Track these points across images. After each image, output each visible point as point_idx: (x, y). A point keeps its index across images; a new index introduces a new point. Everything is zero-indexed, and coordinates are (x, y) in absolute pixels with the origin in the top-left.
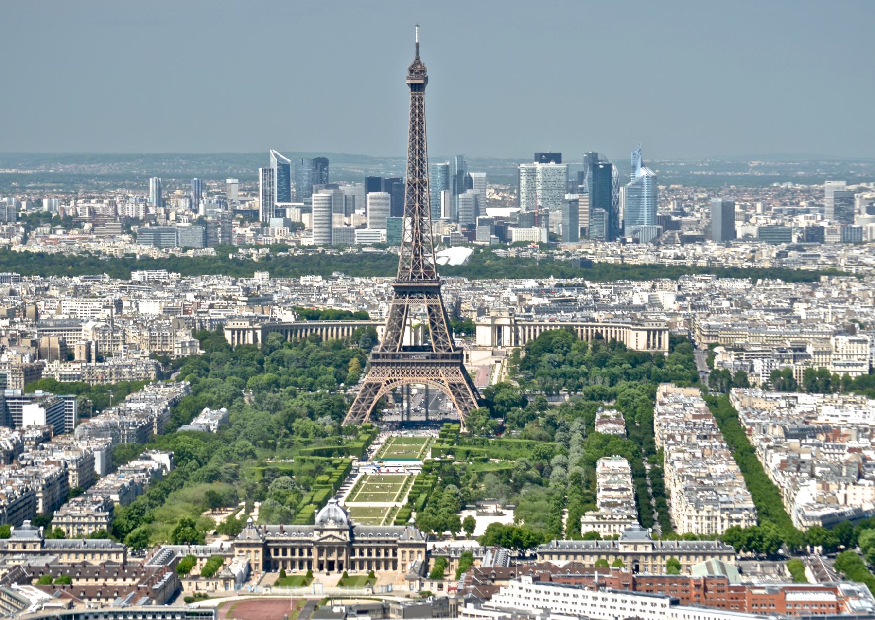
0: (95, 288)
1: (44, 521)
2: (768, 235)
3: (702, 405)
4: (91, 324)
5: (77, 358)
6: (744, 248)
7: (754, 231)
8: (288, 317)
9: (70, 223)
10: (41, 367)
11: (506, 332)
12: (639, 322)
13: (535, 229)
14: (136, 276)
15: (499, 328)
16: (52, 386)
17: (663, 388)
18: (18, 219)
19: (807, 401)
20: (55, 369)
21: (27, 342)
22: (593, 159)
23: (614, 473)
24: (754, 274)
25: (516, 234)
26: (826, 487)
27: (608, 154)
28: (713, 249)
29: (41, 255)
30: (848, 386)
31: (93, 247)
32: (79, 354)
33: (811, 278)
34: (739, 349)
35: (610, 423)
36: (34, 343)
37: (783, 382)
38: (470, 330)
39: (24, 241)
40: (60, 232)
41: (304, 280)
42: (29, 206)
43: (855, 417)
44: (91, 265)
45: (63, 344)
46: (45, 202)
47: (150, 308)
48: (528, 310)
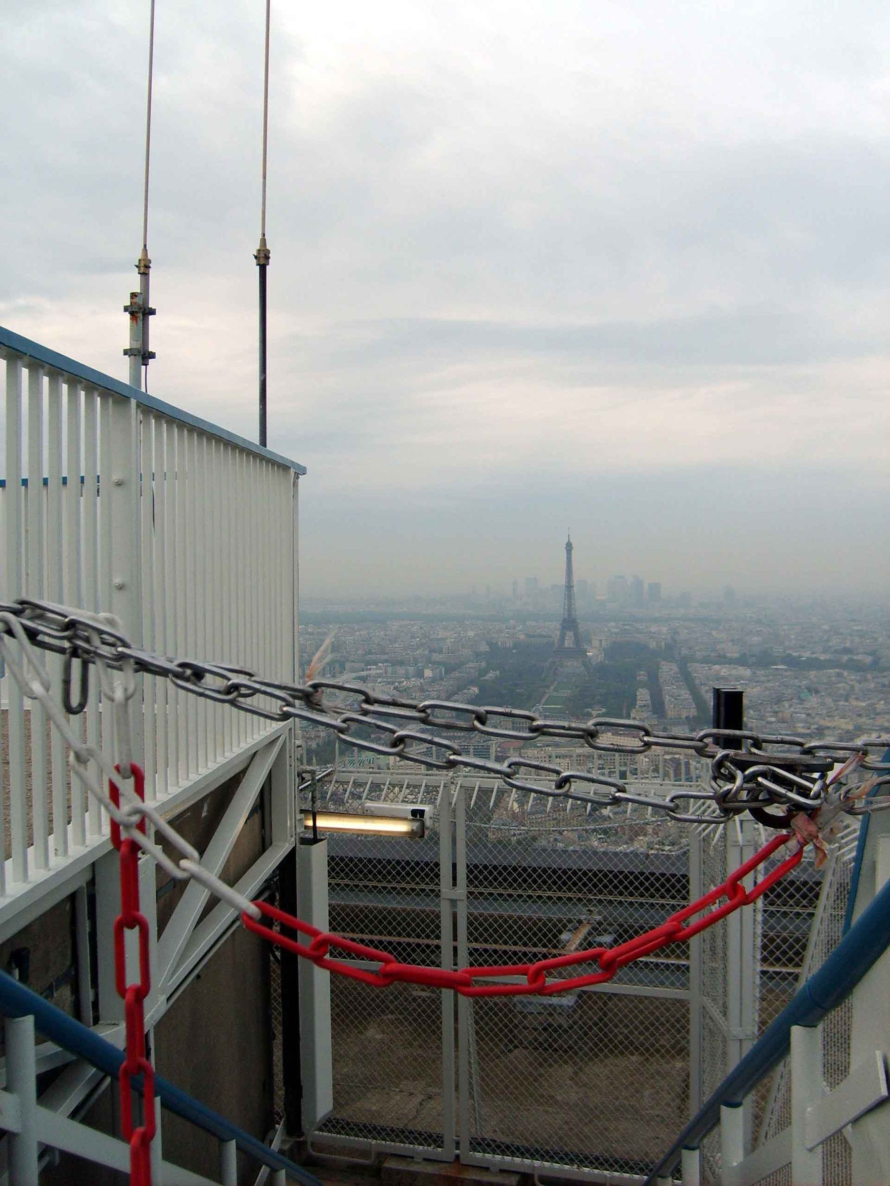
8: (522, 637)
11: (604, 643)
15: (601, 641)
17: (663, 663)
20: (436, 657)
23: (643, 695)
35: (642, 676)
37: (706, 661)
38: (590, 642)
43: (734, 672)
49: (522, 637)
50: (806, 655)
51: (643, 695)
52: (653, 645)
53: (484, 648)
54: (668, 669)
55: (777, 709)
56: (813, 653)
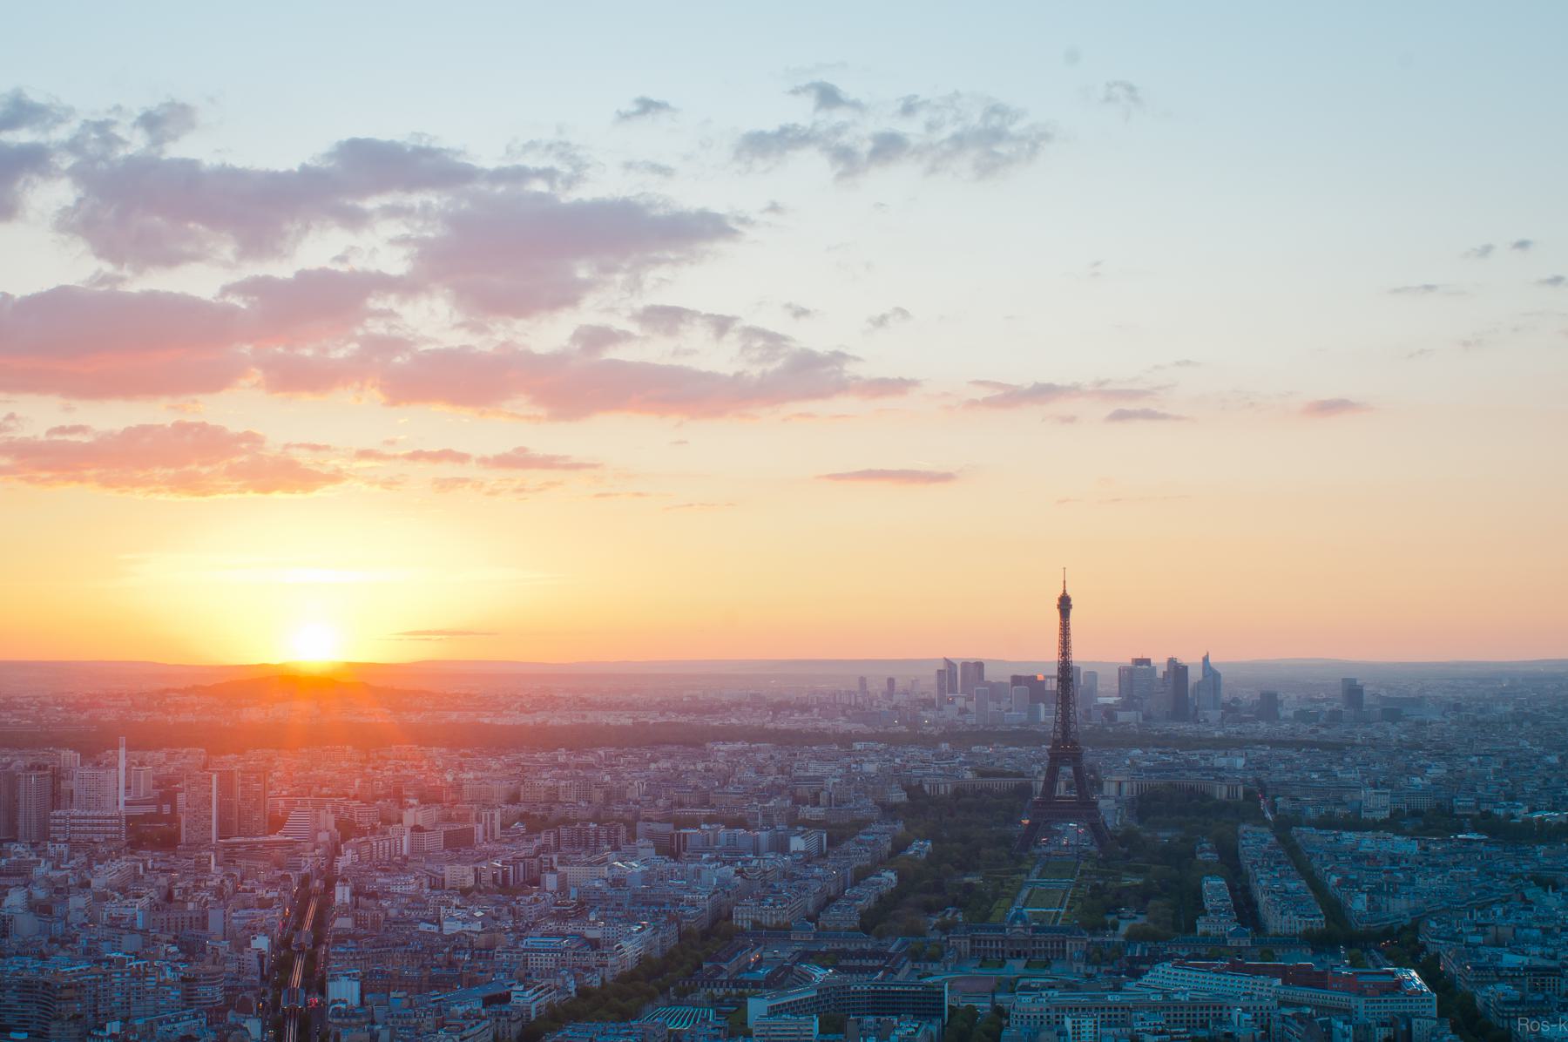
2: (1302, 716)
3: (1273, 839)
6: (1286, 726)
7: (1291, 714)
8: (969, 775)
11: (1126, 787)
12: (1222, 779)
13: (1133, 713)
14: (858, 746)
15: (1120, 784)
17: (1243, 827)
19: (1349, 837)
20: (808, 812)
22: (1171, 661)
23: (1214, 888)
24: (1296, 744)
25: (1122, 716)
26: (1371, 900)
27: (1183, 659)
28: (1263, 725)
30: (1375, 826)
33: (1338, 748)
34: (1294, 799)
35: (1207, 854)
37: (1326, 823)
41: (975, 749)
43: (1386, 847)
44: (821, 737)
47: (871, 768)
48: (1139, 770)
49: (969, 775)
50: (1522, 812)
51: (1214, 888)
52: (1221, 792)
53: (898, 796)
54: (1254, 840)
55: (1482, 921)
56: (1533, 810)
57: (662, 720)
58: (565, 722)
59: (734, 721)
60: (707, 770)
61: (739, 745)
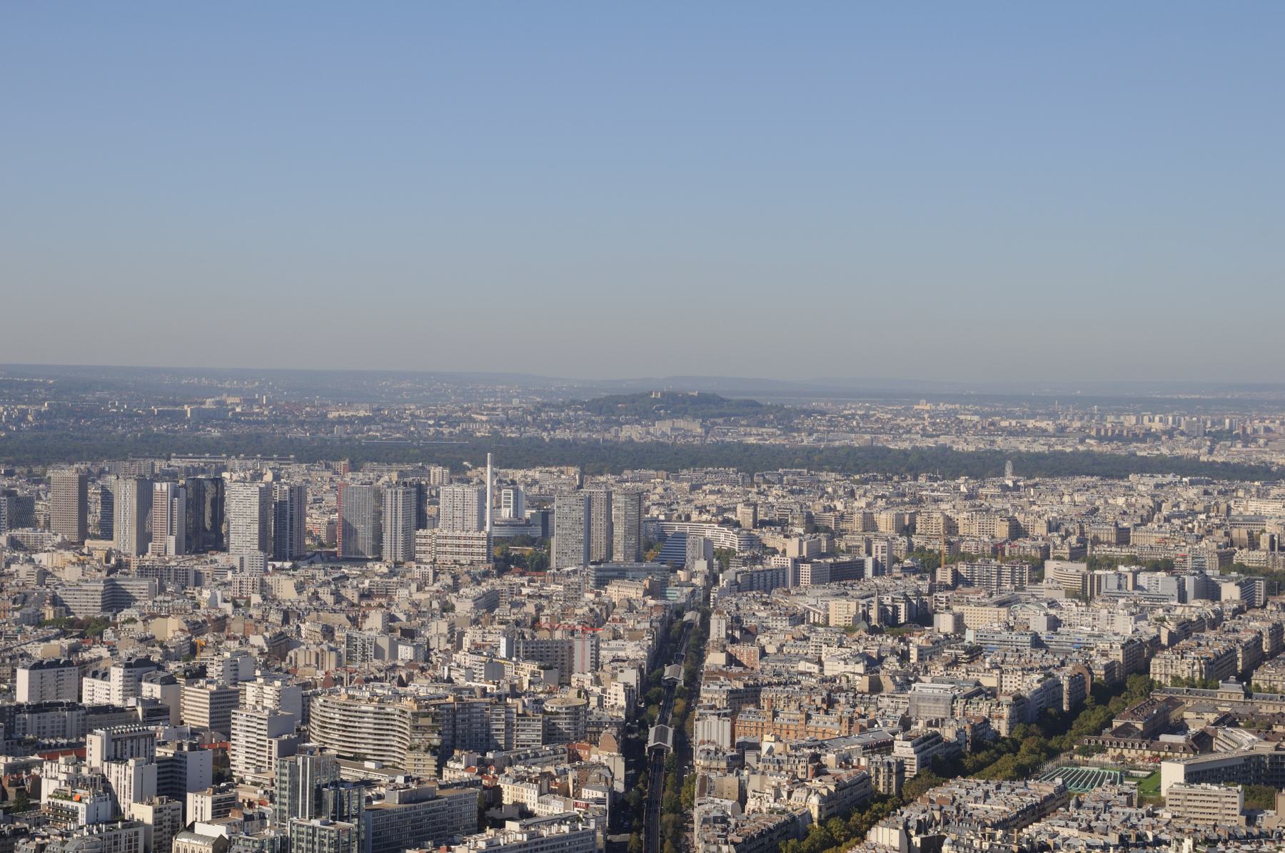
0: (1275, 491)
1: (1244, 677)
4: (1274, 520)
5: (1262, 547)
9: (1247, 439)
10: (1233, 554)
16: (1242, 569)
18: (1205, 434)
21: (1221, 532)
29: (1223, 463)
31: (1267, 458)
32: (1264, 542)
36: (1227, 534)
39: (1211, 452)
40: (1239, 446)
42: (1213, 424)
45: (1250, 534)
46: (1227, 421)
57: (1081, 448)
58: (971, 448)
59: (1165, 451)
60: (1129, 505)
61: (1170, 478)
